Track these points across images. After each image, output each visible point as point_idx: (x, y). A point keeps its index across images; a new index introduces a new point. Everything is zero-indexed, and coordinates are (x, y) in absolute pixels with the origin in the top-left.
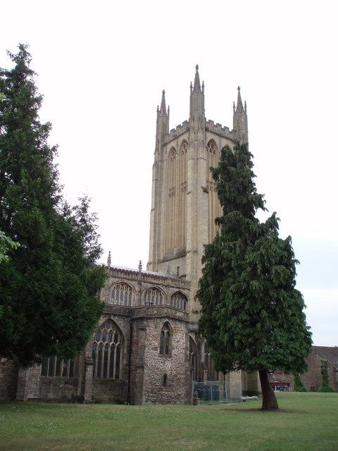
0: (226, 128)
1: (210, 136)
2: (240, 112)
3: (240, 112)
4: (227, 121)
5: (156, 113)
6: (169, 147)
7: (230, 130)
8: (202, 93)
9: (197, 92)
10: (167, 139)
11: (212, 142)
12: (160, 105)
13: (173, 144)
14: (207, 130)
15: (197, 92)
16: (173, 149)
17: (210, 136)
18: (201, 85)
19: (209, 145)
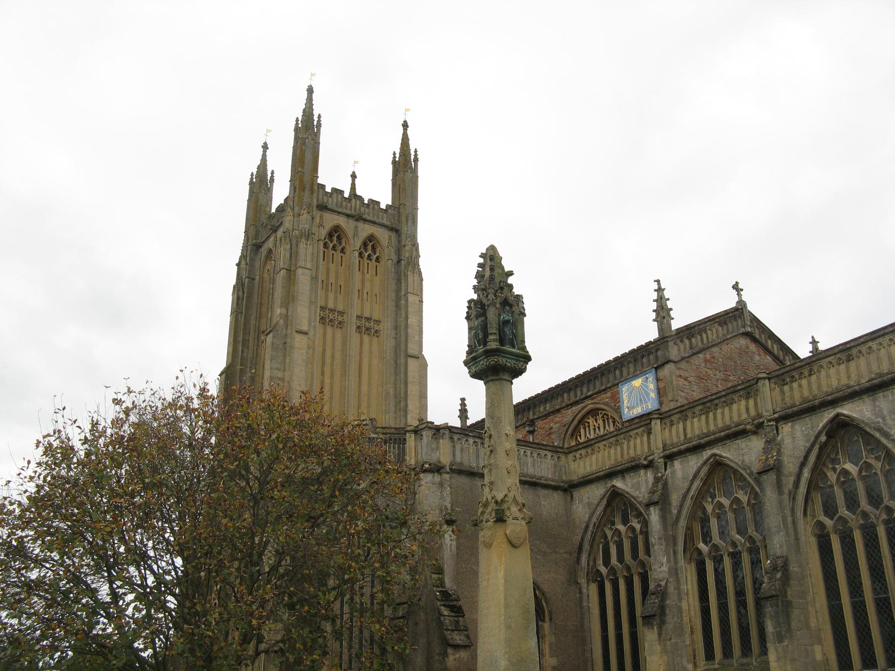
0: (335, 190)
1: (332, 221)
2: (405, 169)
3: (405, 169)
4: (378, 189)
5: (248, 187)
6: (264, 251)
7: (383, 206)
8: (415, 172)
9: (307, 134)
10: (264, 234)
11: (336, 233)
12: (255, 171)
13: (270, 244)
14: (323, 208)
15: (307, 134)
16: (270, 251)
17: (332, 221)
18: (412, 157)
19: (330, 235)
